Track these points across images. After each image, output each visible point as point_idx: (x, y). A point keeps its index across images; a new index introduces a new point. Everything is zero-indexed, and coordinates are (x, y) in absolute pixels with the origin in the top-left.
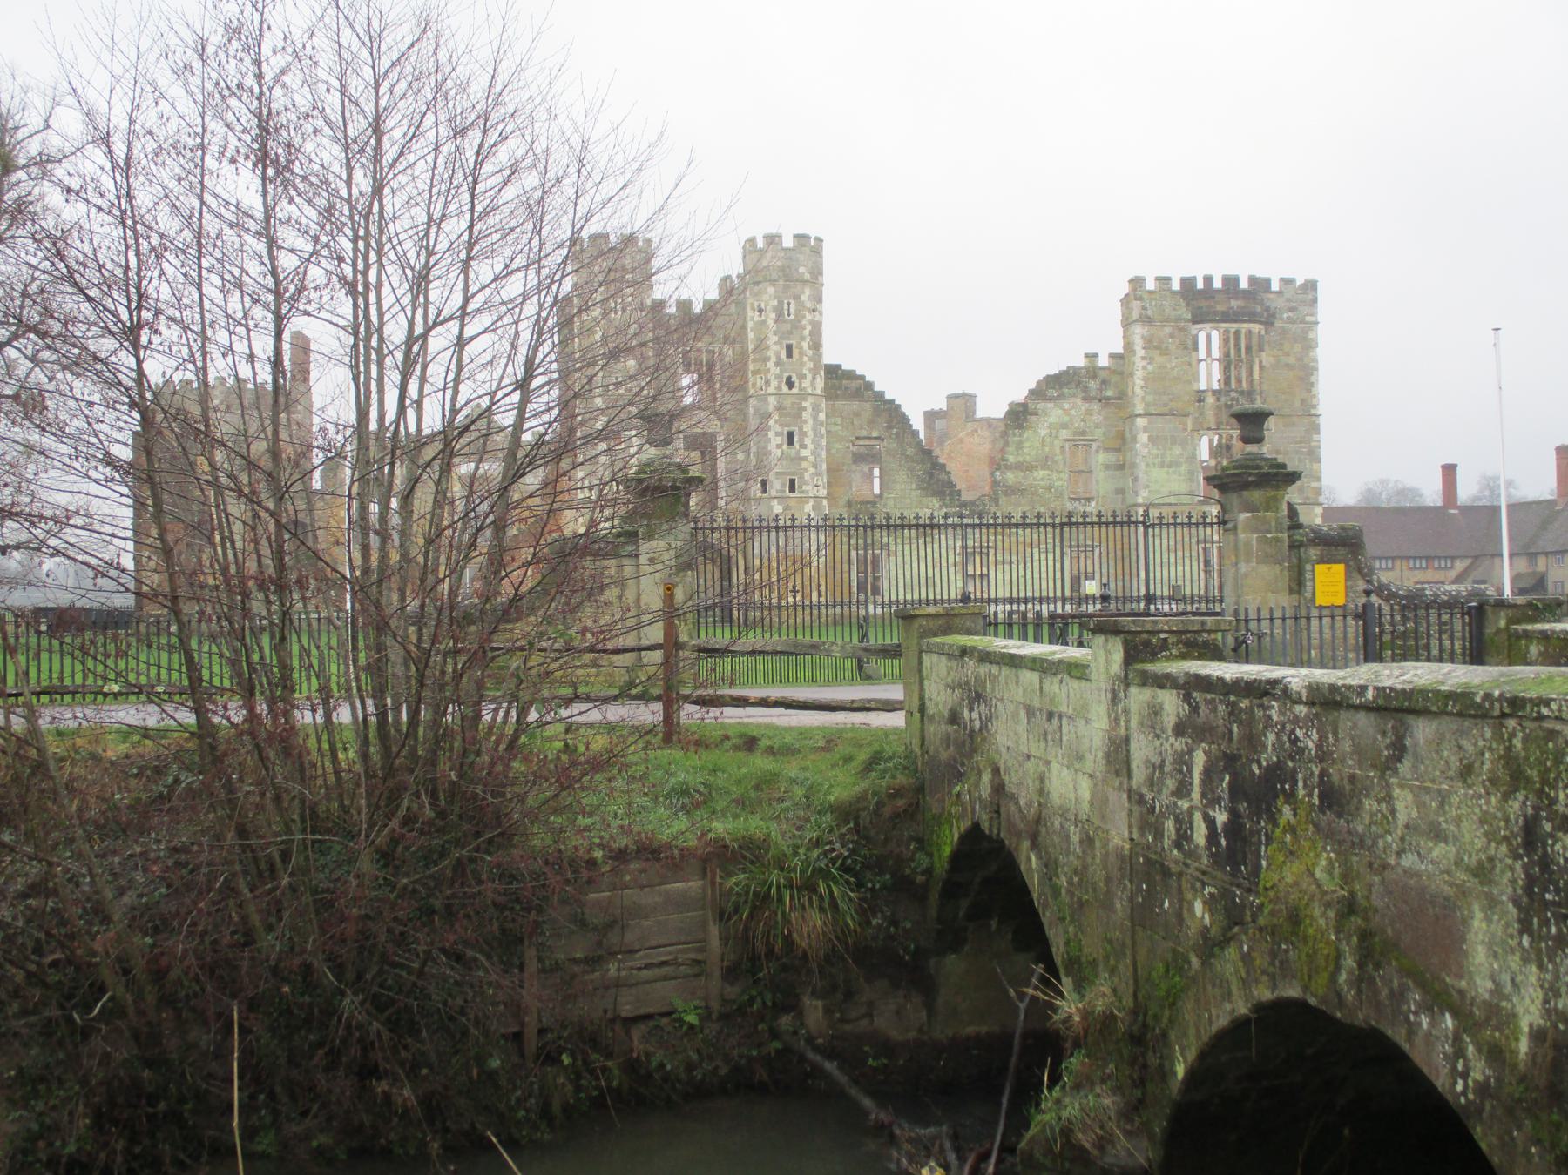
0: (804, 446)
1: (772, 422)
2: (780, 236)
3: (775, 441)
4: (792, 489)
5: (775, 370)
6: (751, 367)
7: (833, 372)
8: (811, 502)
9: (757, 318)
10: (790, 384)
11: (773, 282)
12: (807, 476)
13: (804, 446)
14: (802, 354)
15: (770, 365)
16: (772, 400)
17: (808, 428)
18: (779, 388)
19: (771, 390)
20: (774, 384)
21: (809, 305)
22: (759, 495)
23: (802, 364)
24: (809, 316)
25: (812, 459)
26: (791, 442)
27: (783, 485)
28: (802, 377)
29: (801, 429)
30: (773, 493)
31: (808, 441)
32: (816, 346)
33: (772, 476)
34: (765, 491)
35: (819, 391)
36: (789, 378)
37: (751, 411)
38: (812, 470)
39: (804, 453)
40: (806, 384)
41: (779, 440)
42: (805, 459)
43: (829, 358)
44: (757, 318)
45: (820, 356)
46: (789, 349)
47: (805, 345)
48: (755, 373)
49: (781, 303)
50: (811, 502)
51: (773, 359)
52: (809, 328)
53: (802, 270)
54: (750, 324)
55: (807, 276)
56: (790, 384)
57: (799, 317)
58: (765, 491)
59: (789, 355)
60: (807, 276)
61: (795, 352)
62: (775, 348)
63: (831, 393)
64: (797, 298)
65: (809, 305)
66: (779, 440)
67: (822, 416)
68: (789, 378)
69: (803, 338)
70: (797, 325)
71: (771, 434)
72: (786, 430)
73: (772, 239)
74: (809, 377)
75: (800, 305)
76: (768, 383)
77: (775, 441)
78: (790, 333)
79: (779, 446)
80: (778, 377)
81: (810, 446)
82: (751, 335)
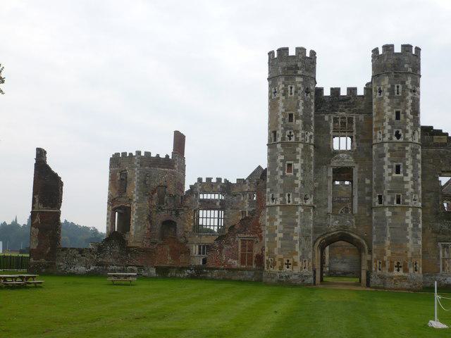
0: (406, 175)
1: (385, 159)
2: (393, 46)
3: (388, 171)
4: (398, 202)
5: (389, 127)
6: (374, 127)
7: (428, 130)
8: (411, 210)
9: (378, 96)
10: (398, 136)
11: (388, 74)
12: (408, 194)
13: (406, 175)
14: (406, 117)
15: (386, 124)
16: (386, 145)
17: (408, 163)
18: (391, 139)
19: (386, 139)
20: (388, 136)
21: (410, 87)
22: (377, 204)
23: (406, 124)
24: (410, 95)
25: (412, 183)
26: (398, 172)
27: (392, 199)
28: (406, 131)
29: (404, 164)
30: (386, 204)
31: (409, 172)
32: (416, 112)
33: (385, 192)
34: (380, 203)
35: (417, 141)
36: (397, 132)
37: (374, 153)
38: (412, 190)
39: (406, 179)
40: (408, 136)
41: (390, 171)
42: (407, 182)
43: (425, 121)
44: (378, 96)
45: (418, 119)
46: (398, 114)
47: (408, 112)
48: (377, 129)
49: (393, 86)
50: (411, 210)
51: (387, 121)
52: (411, 101)
53: (406, 66)
54: (374, 100)
55: (410, 70)
56: (398, 136)
57: (404, 96)
58: (380, 202)
59: (398, 117)
60: (410, 70)
61: (402, 116)
62: (389, 113)
63: (424, 144)
64: (403, 83)
65: (410, 87)
66: (390, 171)
67: (419, 157)
68: (397, 132)
69: (406, 108)
70: (403, 99)
71: (385, 167)
72: (395, 164)
73: (389, 48)
74: (410, 132)
75: (405, 87)
76: (384, 136)
77: (388, 171)
78: (399, 104)
79: (390, 174)
80: (390, 131)
81: (411, 175)
82: (374, 107)
